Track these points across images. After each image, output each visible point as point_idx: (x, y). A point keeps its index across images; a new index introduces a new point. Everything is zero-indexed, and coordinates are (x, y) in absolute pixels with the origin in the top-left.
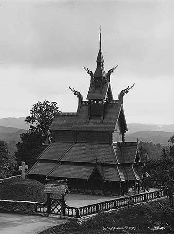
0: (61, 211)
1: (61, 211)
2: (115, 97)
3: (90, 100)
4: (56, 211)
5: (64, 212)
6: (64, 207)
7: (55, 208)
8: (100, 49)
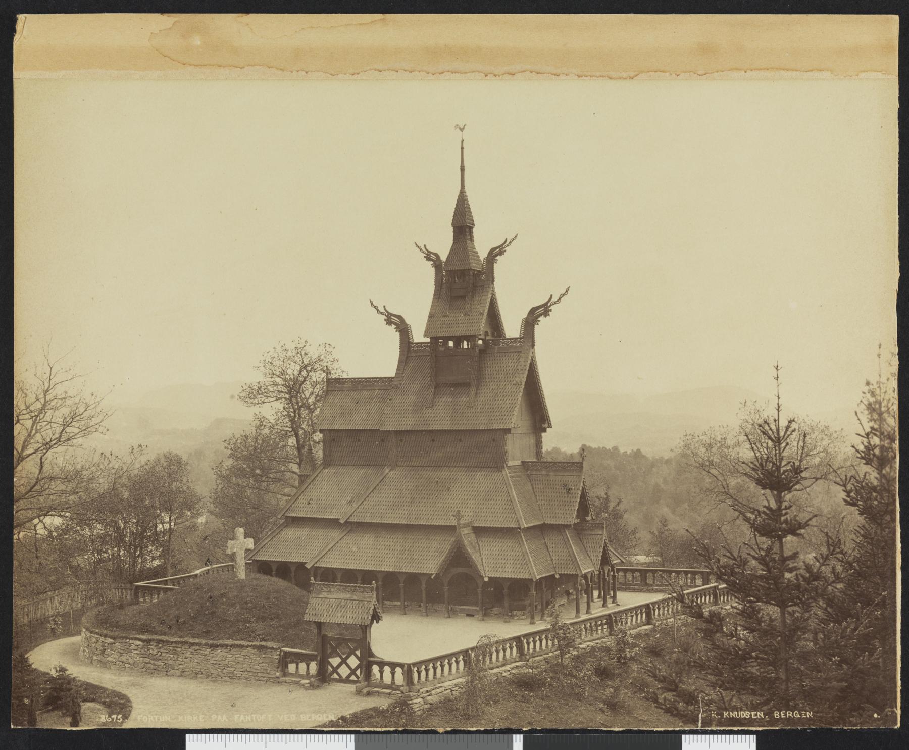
0: (358, 672)
1: (358, 672)
2: (512, 328)
3: (434, 340)
4: (344, 671)
5: (368, 674)
6: (368, 661)
7: (340, 665)
8: (463, 186)
